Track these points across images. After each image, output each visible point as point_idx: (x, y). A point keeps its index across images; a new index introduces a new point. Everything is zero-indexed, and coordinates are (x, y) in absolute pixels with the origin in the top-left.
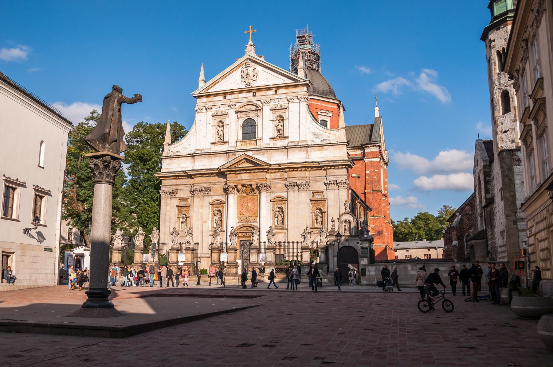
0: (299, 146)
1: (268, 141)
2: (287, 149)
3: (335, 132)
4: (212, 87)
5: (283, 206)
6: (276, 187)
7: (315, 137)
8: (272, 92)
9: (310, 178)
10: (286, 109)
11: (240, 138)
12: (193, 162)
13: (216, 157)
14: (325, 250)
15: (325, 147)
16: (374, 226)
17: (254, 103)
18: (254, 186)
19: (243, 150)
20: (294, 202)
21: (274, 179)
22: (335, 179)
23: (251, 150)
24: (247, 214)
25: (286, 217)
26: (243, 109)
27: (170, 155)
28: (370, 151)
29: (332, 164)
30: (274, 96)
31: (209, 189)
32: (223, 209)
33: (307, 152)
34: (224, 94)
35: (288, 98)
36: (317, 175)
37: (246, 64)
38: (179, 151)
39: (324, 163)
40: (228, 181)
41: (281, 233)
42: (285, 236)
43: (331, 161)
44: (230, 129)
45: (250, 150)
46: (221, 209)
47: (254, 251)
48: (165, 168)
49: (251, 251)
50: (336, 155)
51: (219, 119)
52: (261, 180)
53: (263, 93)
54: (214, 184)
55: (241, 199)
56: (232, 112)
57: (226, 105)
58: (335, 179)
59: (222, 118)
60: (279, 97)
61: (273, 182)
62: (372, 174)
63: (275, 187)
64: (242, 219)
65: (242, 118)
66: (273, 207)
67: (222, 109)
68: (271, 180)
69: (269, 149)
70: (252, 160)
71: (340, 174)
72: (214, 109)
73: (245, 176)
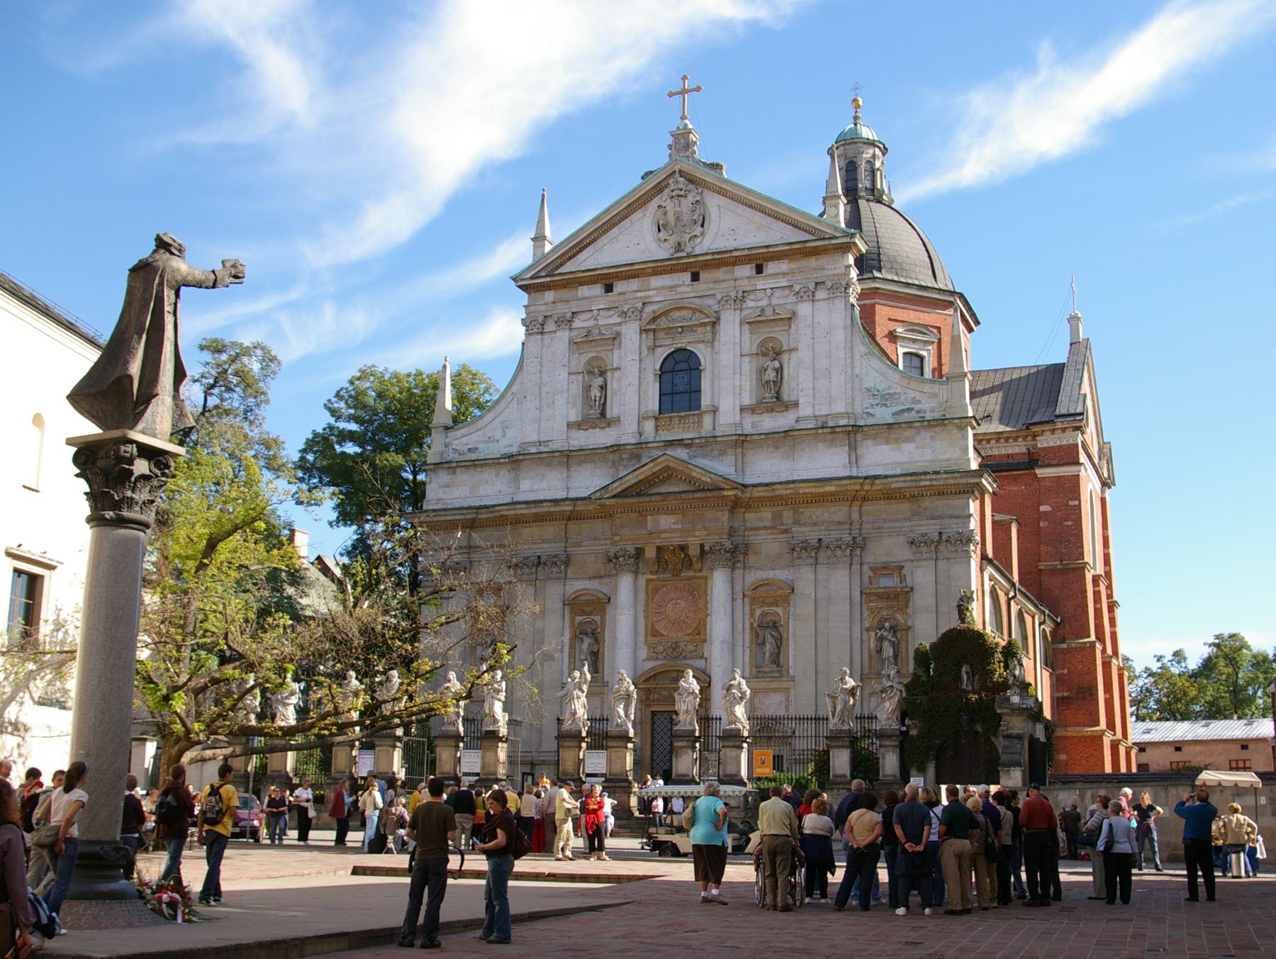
4: (570, 258)
5: (780, 611)
6: (760, 553)
7: (878, 402)
8: (746, 271)
10: (790, 318)
11: (653, 404)
12: (516, 481)
13: (584, 465)
14: (897, 743)
16: (1065, 671)
17: (693, 303)
18: (694, 551)
23: (686, 442)
24: (674, 635)
27: (449, 459)
28: (1052, 444)
29: (928, 483)
33: (853, 447)
34: (607, 280)
35: (797, 288)
37: (672, 188)
38: (477, 448)
39: (904, 481)
41: (775, 690)
42: (787, 699)
43: (925, 473)
45: (679, 443)
46: (597, 618)
47: (685, 743)
48: (435, 497)
49: (677, 744)
50: (940, 457)
53: (720, 274)
54: (578, 545)
55: (652, 590)
56: (631, 333)
57: (611, 313)
59: (599, 349)
62: (1058, 514)
64: (660, 649)
65: (659, 350)
66: (752, 615)
67: (600, 323)
69: (741, 442)
71: (950, 512)
72: (577, 323)
73: (666, 521)
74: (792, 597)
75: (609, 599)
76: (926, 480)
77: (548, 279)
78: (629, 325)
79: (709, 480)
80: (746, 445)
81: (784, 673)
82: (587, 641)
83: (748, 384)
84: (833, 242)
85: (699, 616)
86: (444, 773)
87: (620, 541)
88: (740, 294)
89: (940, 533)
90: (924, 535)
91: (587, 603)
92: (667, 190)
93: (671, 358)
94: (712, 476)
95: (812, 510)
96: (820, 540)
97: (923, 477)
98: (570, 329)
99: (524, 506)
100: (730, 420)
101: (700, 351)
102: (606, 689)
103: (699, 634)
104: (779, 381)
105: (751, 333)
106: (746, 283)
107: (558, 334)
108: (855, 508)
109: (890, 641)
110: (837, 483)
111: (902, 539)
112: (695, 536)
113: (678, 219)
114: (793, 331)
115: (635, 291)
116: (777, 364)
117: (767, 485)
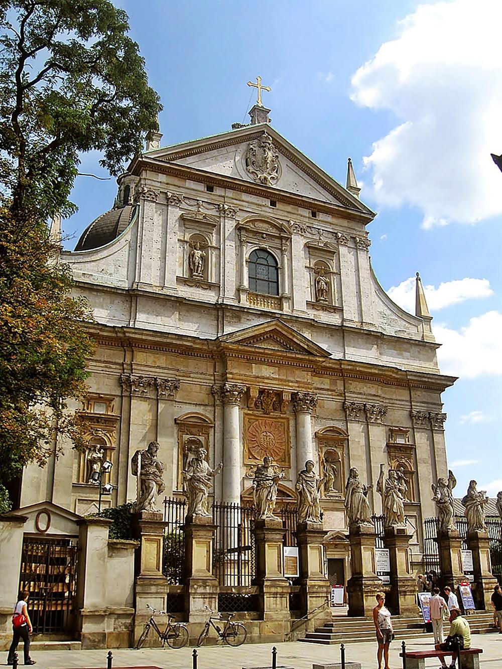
1: (304, 308)
3: (416, 323)
8: (307, 213)
11: (246, 284)
12: (132, 314)
13: (192, 313)
18: (287, 397)
21: (321, 389)
26: (251, 226)
29: (427, 380)
34: (211, 182)
36: (394, 397)
39: (415, 376)
40: (231, 373)
53: (290, 208)
60: (322, 227)
69: (312, 325)
72: (184, 205)
73: (267, 371)
76: (425, 378)
77: (168, 165)
79: (306, 347)
84: (362, 215)
85: (284, 447)
86: (367, 572)
87: (232, 379)
89: (429, 413)
91: (194, 426)
93: (254, 252)
94: (310, 344)
97: (426, 375)
101: (277, 254)
104: (329, 292)
105: (309, 254)
106: (307, 220)
109: (404, 479)
110: (381, 368)
111: (406, 413)
112: (289, 386)
115: (233, 199)
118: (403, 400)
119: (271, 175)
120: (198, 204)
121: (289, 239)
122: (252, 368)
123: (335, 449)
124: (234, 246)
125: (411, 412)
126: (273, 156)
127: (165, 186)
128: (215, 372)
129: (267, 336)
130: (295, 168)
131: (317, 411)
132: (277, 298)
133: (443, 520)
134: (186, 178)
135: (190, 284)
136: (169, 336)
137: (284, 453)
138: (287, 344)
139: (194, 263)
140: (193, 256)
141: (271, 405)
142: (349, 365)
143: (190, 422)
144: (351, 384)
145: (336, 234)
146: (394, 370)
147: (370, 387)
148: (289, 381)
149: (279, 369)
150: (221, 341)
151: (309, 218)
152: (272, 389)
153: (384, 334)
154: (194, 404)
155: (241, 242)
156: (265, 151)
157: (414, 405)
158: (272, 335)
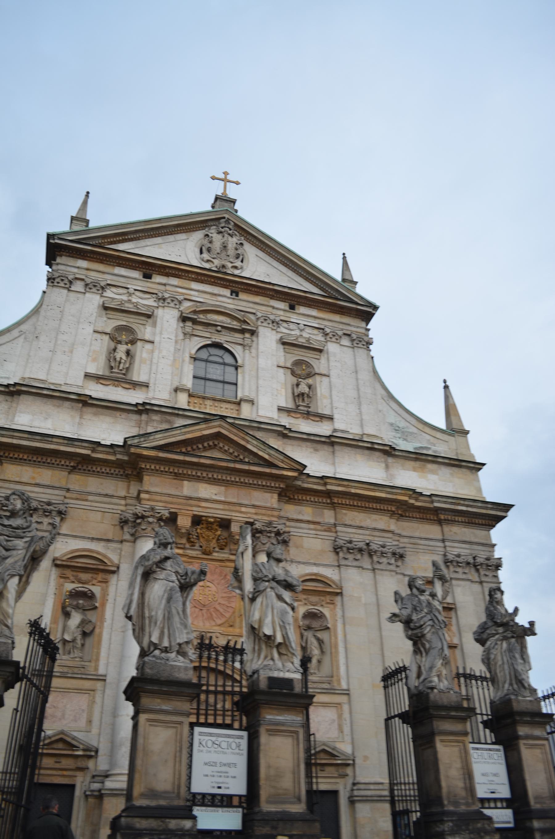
0: (369, 445)
2: (332, 444)
5: (326, 611)
6: (302, 547)
9: (402, 540)
10: (321, 351)
11: (188, 382)
13: (102, 417)
15: (430, 466)
19: (202, 416)
20: (363, 600)
21: (298, 521)
22: (468, 551)
25: (341, 649)
26: (202, 318)
29: (464, 508)
30: (288, 314)
31: (62, 508)
32: (105, 594)
35: (328, 330)
36: (417, 534)
37: (223, 225)
39: (445, 502)
40: (147, 492)
42: (340, 716)
43: (464, 499)
44: (156, 354)
46: (96, 590)
50: (460, 491)
51: (122, 320)
52: (263, 511)
53: (258, 299)
54: (83, 496)
58: (468, 551)
59: (132, 320)
61: (295, 530)
63: (297, 547)
67: (134, 300)
68: (288, 523)
70: (243, 443)
72: (109, 293)
74: (339, 598)
75: (118, 568)
77: (89, 248)
78: (167, 310)
79: (267, 457)
80: (286, 440)
81: (335, 684)
82: (76, 619)
83: (283, 390)
84: (359, 307)
85: (233, 605)
86: (152, 794)
87: (148, 500)
88: (278, 319)
89: (474, 558)
90: (459, 556)
91: (85, 570)
92: (214, 227)
94: (272, 452)
95: (356, 514)
96: (368, 544)
97: (462, 502)
98: (102, 296)
99: (26, 436)
100: (270, 415)
101: (237, 351)
102: (99, 685)
103: (231, 626)
105: (285, 352)
106: (281, 313)
107: (88, 295)
108: (393, 521)
112: (241, 512)
113: (225, 247)
114: (323, 360)
116: (310, 381)
117: (323, 478)
118: (431, 539)
119: (232, 263)
120: (128, 292)
121: (253, 333)
122: (182, 487)
123: (321, 609)
124: (174, 338)
125: (445, 555)
126: (237, 244)
127: (85, 272)
128: (129, 493)
129: (208, 444)
130: (268, 258)
131: (291, 552)
132: (234, 403)
133: (419, 667)
134: (115, 264)
135: (104, 383)
136: (54, 440)
137: (234, 612)
138: (239, 455)
139: (115, 359)
140: (115, 350)
141: (214, 541)
142: (339, 485)
143: (78, 562)
144: (345, 514)
145: (323, 329)
146: (411, 493)
147: (376, 520)
148: (241, 505)
149: (226, 490)
150: (131, 445)
151: (284, 310)
152: (213, 517)
153: (394, 449)
154: (89, 538)
155: (185, 334)
156: (223, 236)
157: (450, 547)
158: (216, 443)
